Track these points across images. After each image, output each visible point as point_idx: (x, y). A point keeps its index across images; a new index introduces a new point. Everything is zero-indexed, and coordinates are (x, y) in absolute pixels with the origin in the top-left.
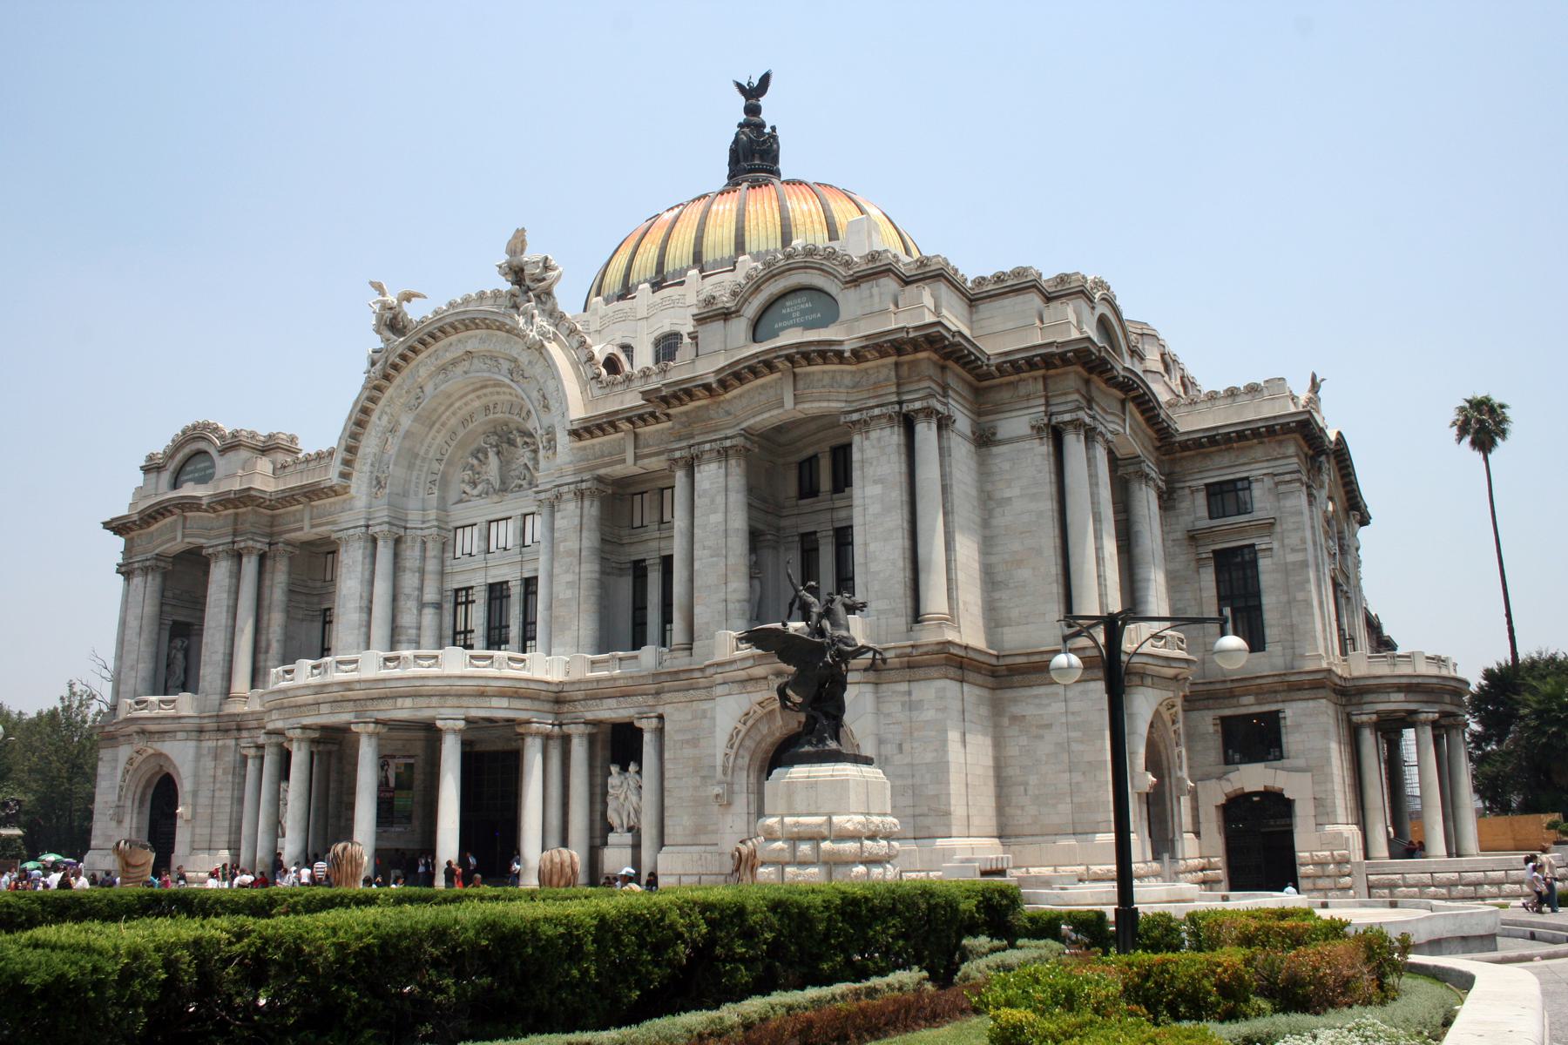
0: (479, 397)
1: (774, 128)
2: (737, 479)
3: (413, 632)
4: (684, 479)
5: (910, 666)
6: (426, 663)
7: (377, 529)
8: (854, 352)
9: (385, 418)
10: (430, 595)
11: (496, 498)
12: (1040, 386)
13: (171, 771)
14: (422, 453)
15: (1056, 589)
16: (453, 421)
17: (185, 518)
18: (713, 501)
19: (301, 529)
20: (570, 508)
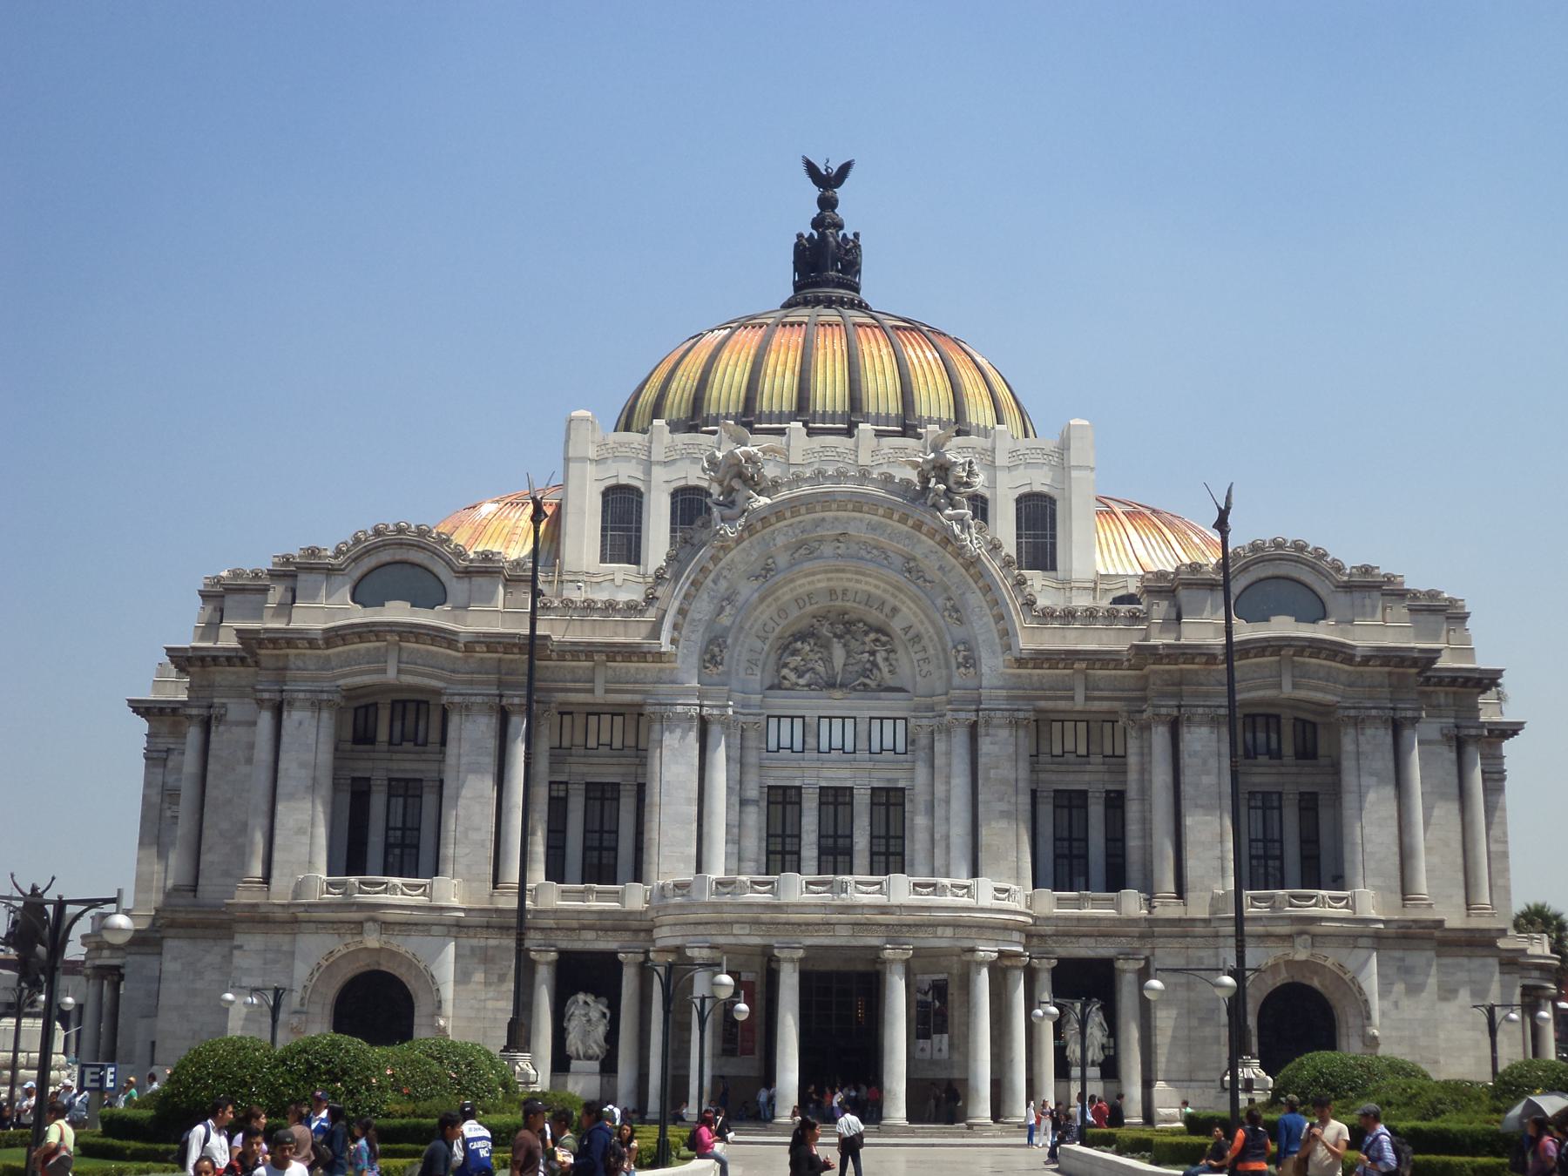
0: (829, 579)
1: (856, 235)
2: (1225, 749)
3: (736, 830)
4: (1167, 735)
5: (1405, 937)
6: (961, 893)
8: (1366, 660)
9: (723, 584)
10: (752, 793)
11: (838, 694)
12: (1451, 701)
13: (400, 972)
14: (747, 627)
15: (1461, 876)
16: (787, 597)
17: (400, 649)
18: (1205, 762)
19: (592, 691)
20: (1004, 733)
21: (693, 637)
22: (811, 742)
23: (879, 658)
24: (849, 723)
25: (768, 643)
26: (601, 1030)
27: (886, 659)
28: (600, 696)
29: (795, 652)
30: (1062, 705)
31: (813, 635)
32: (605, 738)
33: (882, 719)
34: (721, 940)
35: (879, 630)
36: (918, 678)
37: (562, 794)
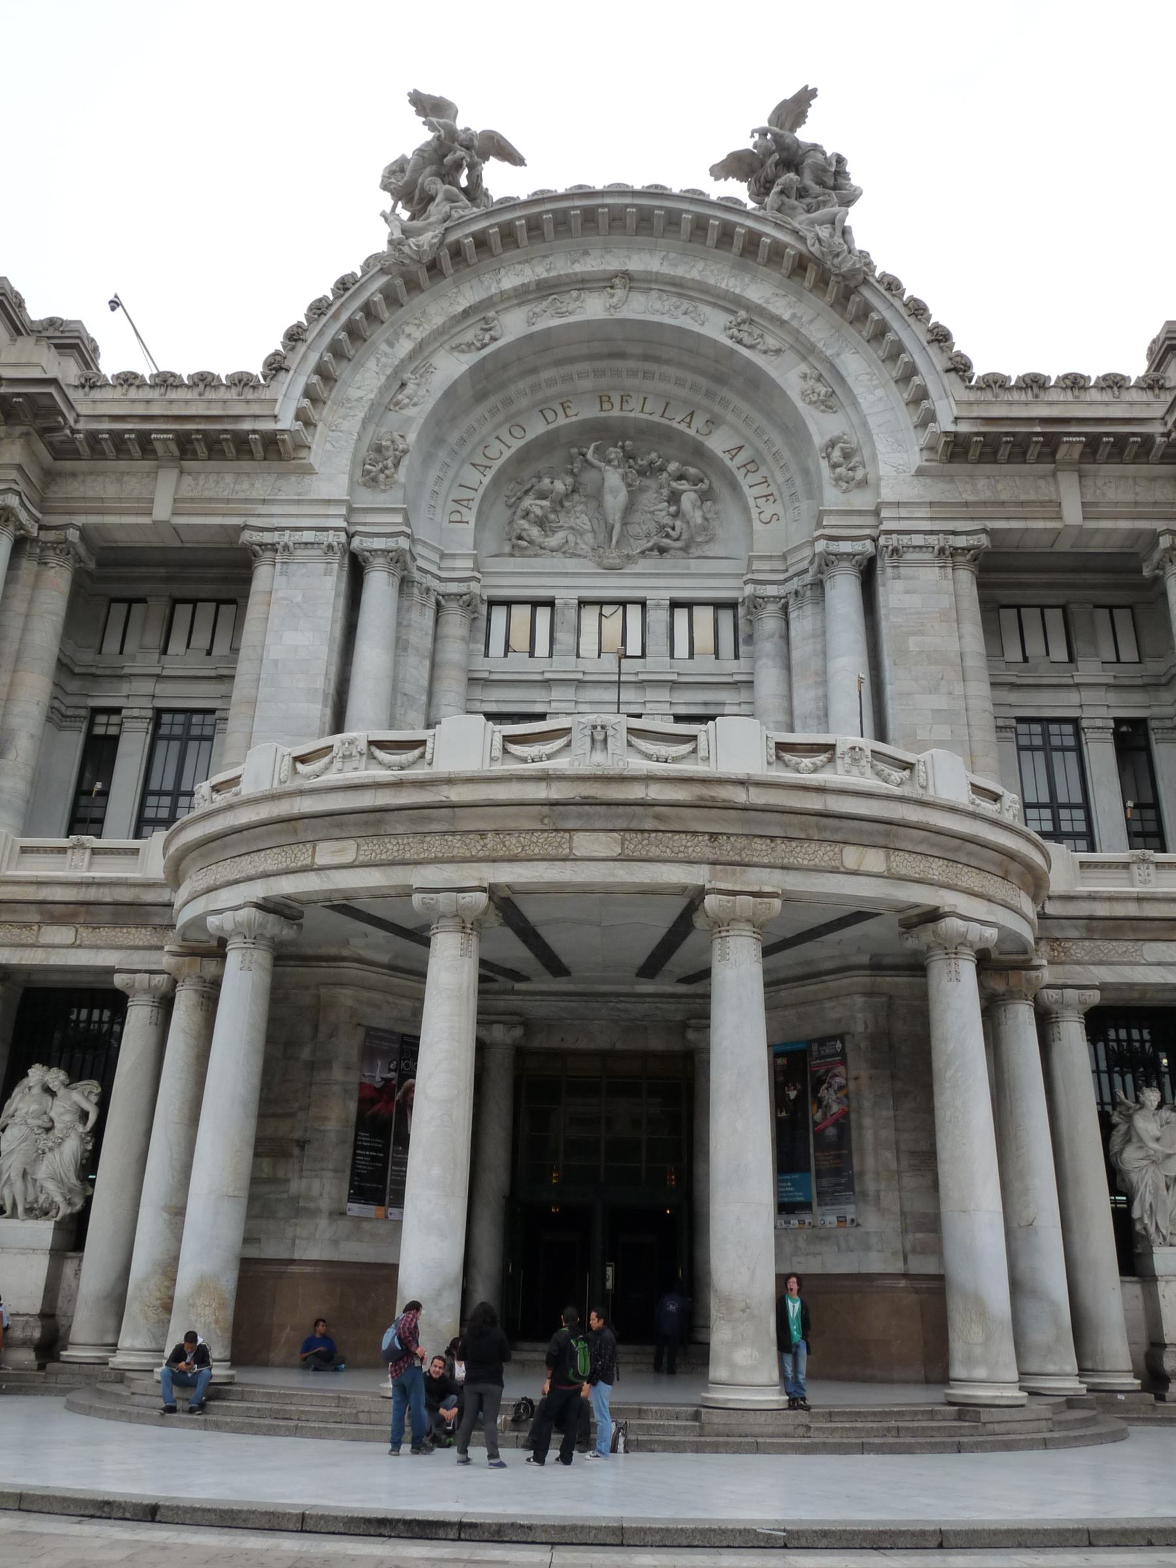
6: (897, 775)
7: (378, 544)
14: (453, 438)
16: (524, 402)
20: (930, 576)
21: (345, 425)
22: (565, 638)
23: (688, 500)
24: (634, 612)
25: (490, 474)
26: (71, 1148)
27: (700, 507)
28: (162, 511)
29: (542, 496)
30: (1040, 524)
31: (572, 473)
32: (201, 640)
33: (689, 605)
34: (287, 886)
35: (685, 463)
36: (757, 525)
37: (112, 731)
